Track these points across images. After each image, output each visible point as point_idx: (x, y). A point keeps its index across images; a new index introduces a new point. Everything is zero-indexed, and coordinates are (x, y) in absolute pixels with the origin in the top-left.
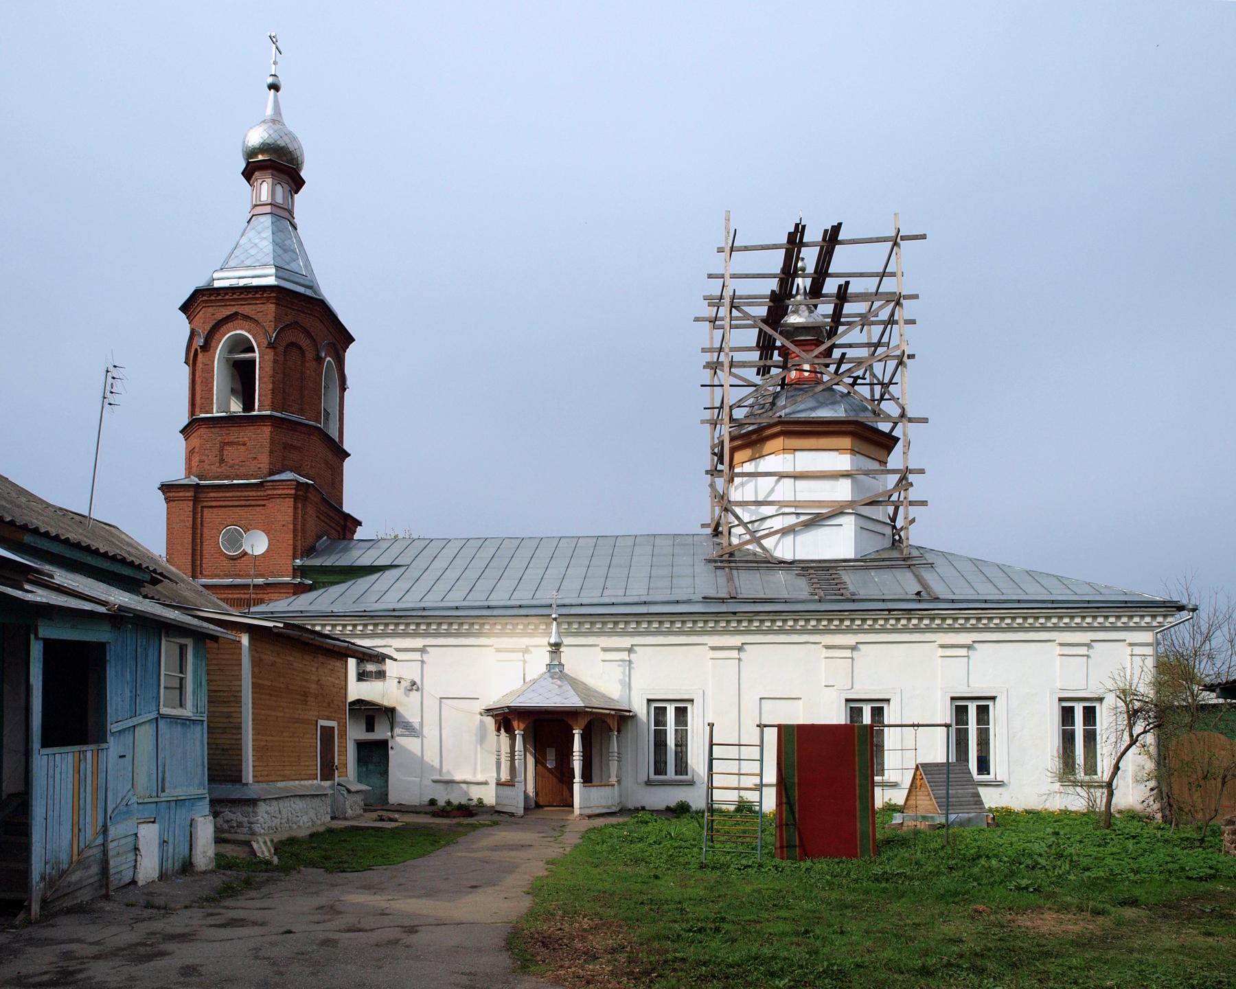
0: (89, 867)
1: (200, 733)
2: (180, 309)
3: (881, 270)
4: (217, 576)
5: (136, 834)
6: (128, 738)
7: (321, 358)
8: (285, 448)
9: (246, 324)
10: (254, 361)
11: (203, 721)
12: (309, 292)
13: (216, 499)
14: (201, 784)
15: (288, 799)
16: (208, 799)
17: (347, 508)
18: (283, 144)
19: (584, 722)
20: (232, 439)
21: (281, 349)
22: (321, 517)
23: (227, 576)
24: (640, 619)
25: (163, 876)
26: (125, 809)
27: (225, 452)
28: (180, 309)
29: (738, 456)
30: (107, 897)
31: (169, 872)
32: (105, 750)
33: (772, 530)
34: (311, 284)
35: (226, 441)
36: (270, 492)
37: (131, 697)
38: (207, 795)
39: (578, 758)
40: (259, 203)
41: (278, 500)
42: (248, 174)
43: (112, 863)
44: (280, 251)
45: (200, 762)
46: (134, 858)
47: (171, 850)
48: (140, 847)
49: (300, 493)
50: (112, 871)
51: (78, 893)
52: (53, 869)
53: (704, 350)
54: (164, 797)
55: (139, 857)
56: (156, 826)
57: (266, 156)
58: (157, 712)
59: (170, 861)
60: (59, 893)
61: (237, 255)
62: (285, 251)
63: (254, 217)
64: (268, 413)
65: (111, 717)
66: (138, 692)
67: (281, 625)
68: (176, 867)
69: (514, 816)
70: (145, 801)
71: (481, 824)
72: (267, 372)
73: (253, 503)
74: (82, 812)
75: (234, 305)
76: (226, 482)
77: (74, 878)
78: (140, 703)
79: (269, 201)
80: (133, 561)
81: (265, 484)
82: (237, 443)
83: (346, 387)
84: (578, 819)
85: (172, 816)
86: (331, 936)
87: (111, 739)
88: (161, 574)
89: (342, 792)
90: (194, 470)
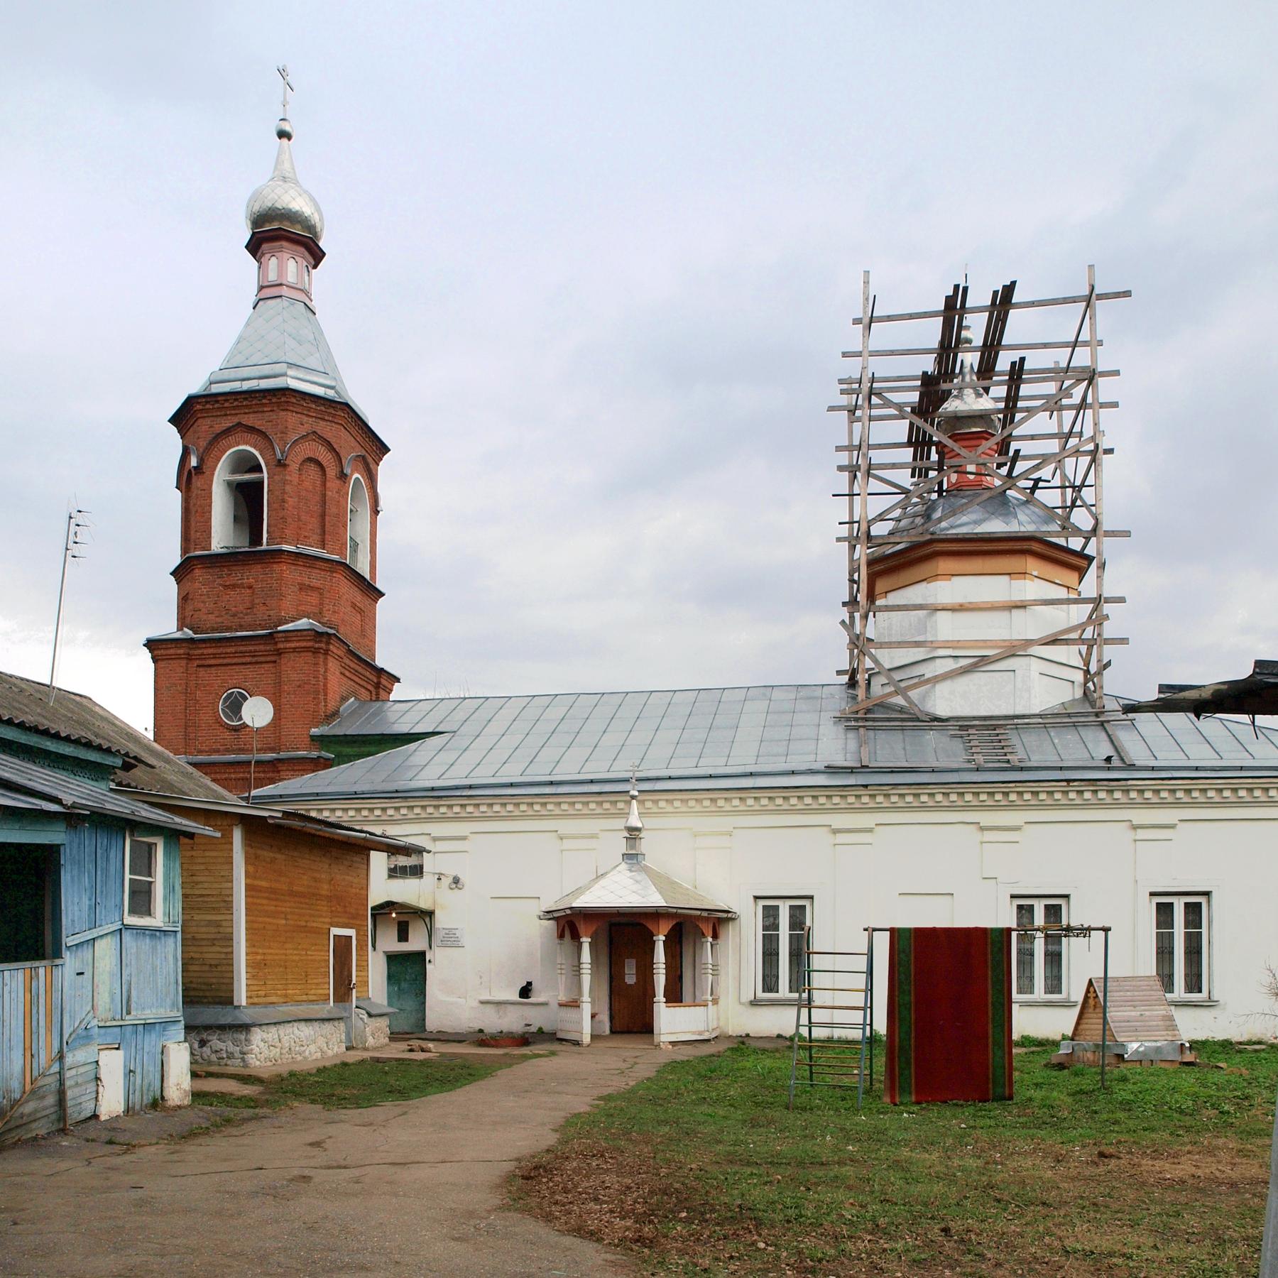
0: (43, 1097)
1: (173, 945)
2: (169, 421)
4: (217, 751)
5: (97, 1062)
6: (86, 953)
7: (346, 475)
9: (248, 436)
10: (260, 484)
11: (176, 932)
13: (215, 656)
14: (174, 1005)
16: (183, 1022)
17: (380, 662)
22: (347, 673)
23: (228, 751)
24: (743, 795)
25: (128, 1110)
26: (84, 1033)
28: (169, 421)
30: (63, 1131)
32: (60, 967)
35: (228, 583)
37: (90, 906)
38: (182, 1018)
41: (291, 654)
43: (69, 1094)
45: (172, 980)
46: (95, 1089)
47: (139, 1081)
48: (102, 1077)
50: (69, 1103)
51: (34, 1125)
52: (4, 1098)
54: (129, 1020)
55: (101, 1089)
56: (120, 1053)
58: (120, 923)
59: (138, 1093)
60: (13, 1124)
65: (66, 929)
66: (98, 900)
67: (280, 815)
68: (145, 1102)
70: (108, 1024)
74: (35, 1037)
75: (237, 414)
76: (227, 634)
77: (28, 1108)
78: (101, 913)
82: (242, 586)
83: (379, 509)
85: (139, 1042)
87: (67, 955)
90: (188, 621)
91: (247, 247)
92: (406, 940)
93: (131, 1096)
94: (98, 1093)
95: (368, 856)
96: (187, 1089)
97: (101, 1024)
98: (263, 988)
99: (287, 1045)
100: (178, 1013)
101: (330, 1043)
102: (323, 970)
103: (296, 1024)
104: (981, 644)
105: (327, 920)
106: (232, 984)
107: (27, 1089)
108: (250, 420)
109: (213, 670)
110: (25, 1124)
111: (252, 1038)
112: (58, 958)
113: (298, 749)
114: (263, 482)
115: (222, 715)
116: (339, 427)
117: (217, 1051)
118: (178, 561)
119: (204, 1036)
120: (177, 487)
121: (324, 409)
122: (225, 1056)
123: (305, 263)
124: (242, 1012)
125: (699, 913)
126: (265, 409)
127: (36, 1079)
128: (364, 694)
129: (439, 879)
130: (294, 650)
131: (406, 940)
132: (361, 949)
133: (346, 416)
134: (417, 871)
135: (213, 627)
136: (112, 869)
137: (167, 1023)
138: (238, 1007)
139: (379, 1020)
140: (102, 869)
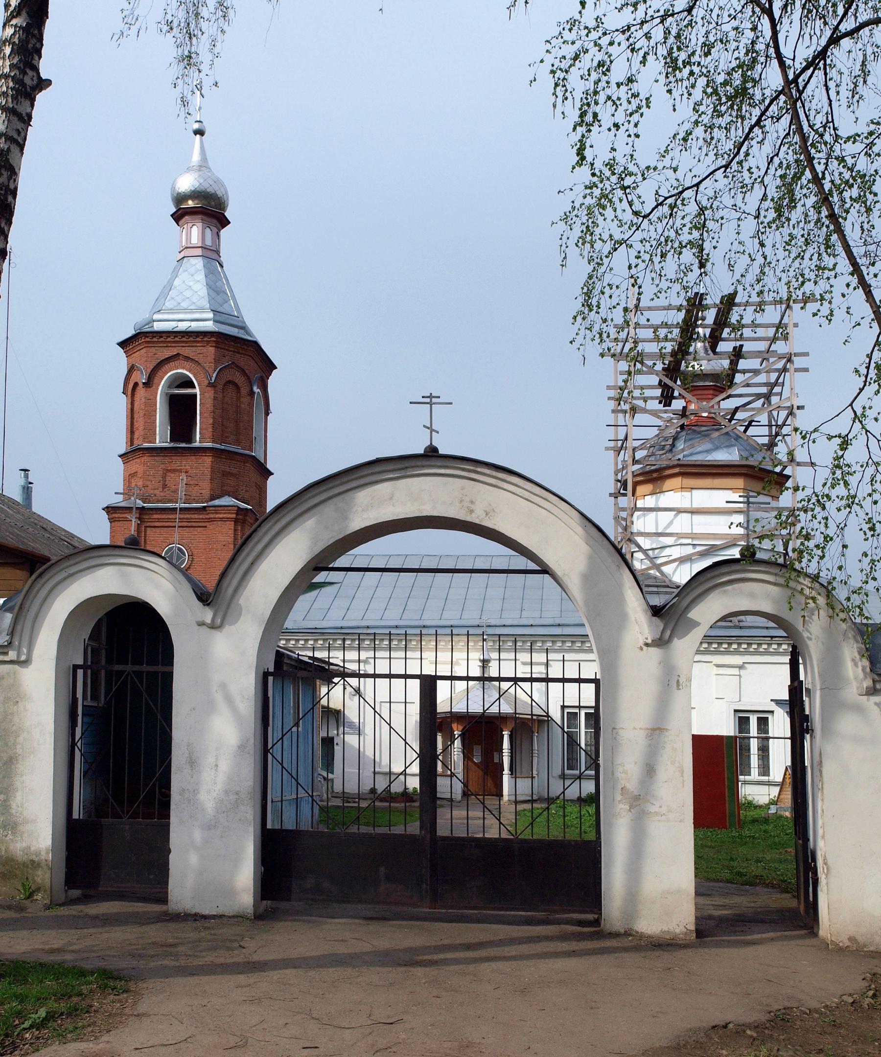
3: (777, 322)
8: (223, 475)
10: (195, 396)
12: (241, 334)
13: (159, 520)
18: (213, 192)
19: (511, 725)
20: (174, 466)
21: (220, 387)
24: (555, 639)
27: (168, 478)
29: (641, 489)
33: (671, 558)
34: (244, 325)
35: (169, 468)
36: (212, 516)
39: (507, 754)
40: (189, 245)
41: (219, 523)
42: (178, 217)
44: (214, 294)
49: (240, 517)
53: (609, 388)
57: (196, 202)
61: (173, 296)
62: (218, 293)
64: (210, 445)
72: (207, 408)
73: (194, 524)
79: (200, 245)
81: (207, 509)
104: (712, 536)
108: (187, 351)
109: (158, 530)
120: (123, 393)
130: (221, 519)
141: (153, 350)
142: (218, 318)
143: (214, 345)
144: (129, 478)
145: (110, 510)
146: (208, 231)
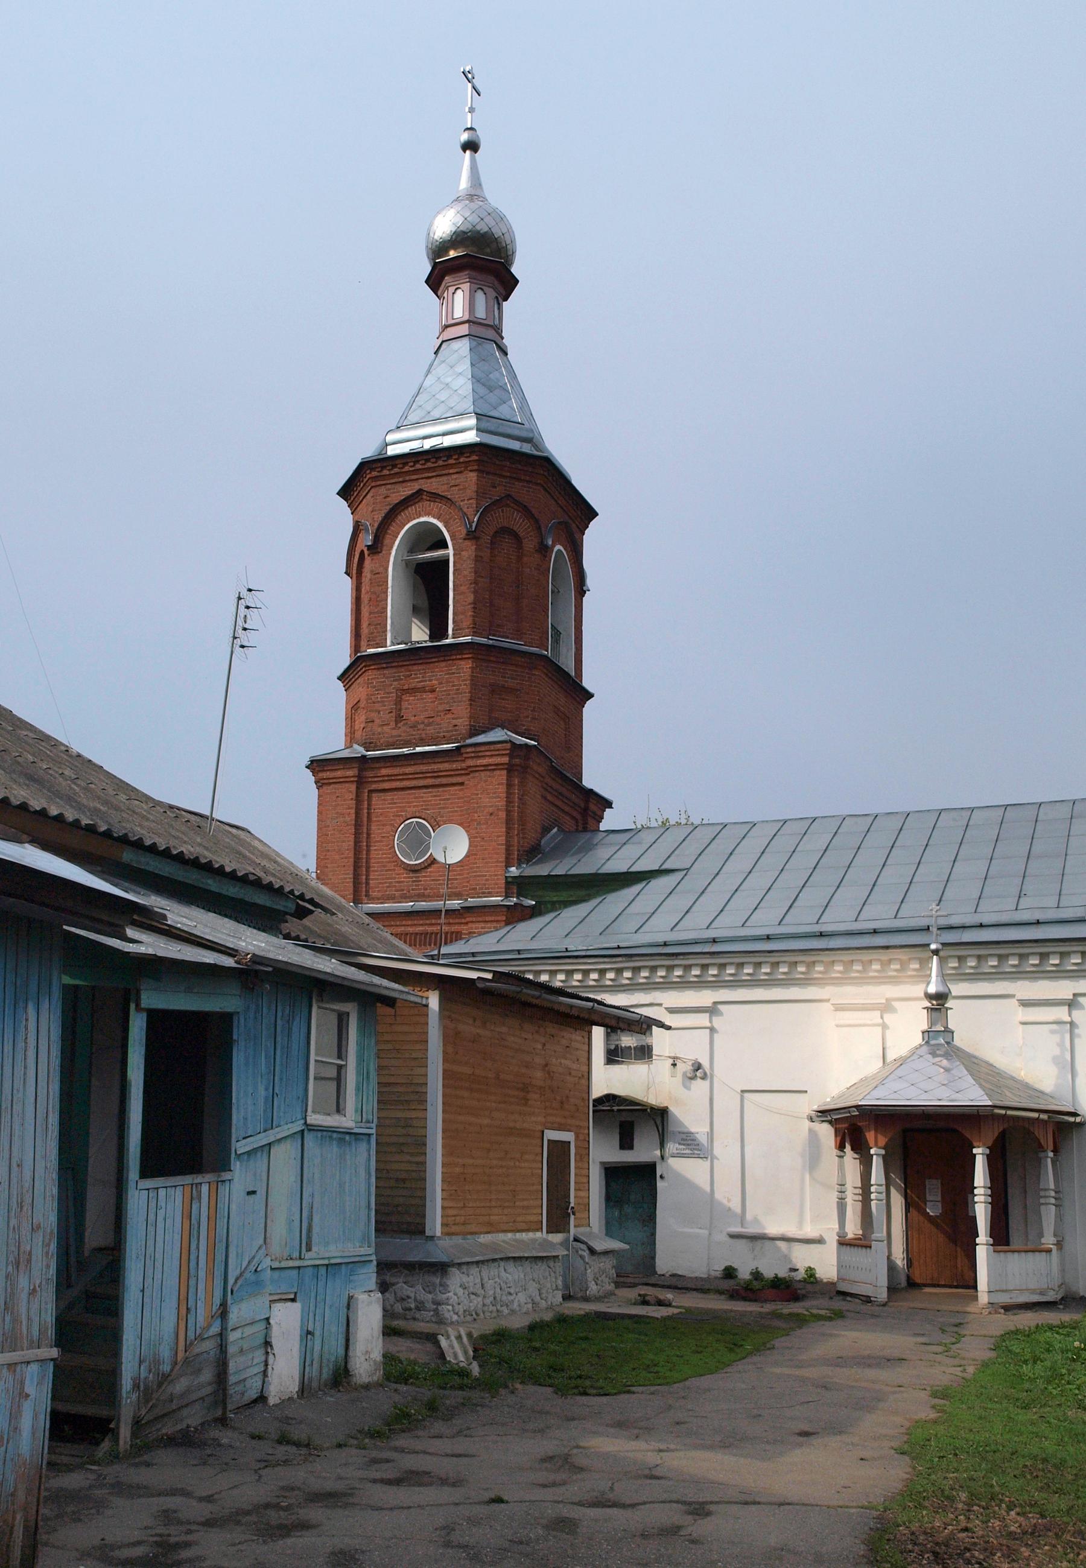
0: (200, 1370)
1: (365, 1155)
2: (338, 494)
5: (268, 1319)
6: (260, 1163)
7: (546, 547)
8: (493, 692)
9: (435, 506)
11: (369, 1135)
12: (527, 448)
14: (365, 1238)
15: (496, 1264)
16: (375, 1263)
17: (588, 782)
18: (486, 229)
20: (414, 683)
21: (486, 539)
22: (549, 797)
25: (304, 1389)
26: (253, 1278)
27: (405, 705)
28: (338, 494)
30: (222, 1421)
31: (315, 1385)
32: (227, 1184)
34: (531, 435)
35: (406, 687)
36: (470, 763)
38: (374, 1258)
40: (451, 322)
41: (482, 774)
42: (435, 282)
43: (232, 1366)
44: (482, 391)
45: (364, 1203)
46: (263, 1358)
47: (317, 1348)
48: (274, 1342)
49: (517, 761)
50: (232, 1379)
51: (185, 1412)
52: (150, 1371)
54: (311, 1258)
55: (271, 1358)
56: (297, 1306)
57: (460, 250)
58: (303, 1122)
59: (316, 1365)
60: (158, 1411)
61: (420, 404)
62: (491, 389)
63: (444, 344)
64: (468, 639)
67: (489, 976)
68: (325, 1376)
69: (871, 1302)
70: (284, 1264)
71: (813, 1315)
72: (465, 576)
73: (444, 781)
74: (192, 1282)
75: (417, 479)
76: (405, 750)
77: (180, 1386)
79: (466, 318)
80: (271, 882)
81: (463, 750)
82: (423, 690)
83: (585, 588)
84: (985, 1312)
85: (321, 1290)
86: (567, 1511)
87: (236, 1165)
88: (311, 901)
89: (580, 1252)
91: (427, 282)
92: (631, 1148)
93: (307, 1369)
94: (266, 1365)
95: (590, 1032)
96: (378, 1359)
97: (276, 1265)
98: (462, 1212)
99: (491, 1292)
100: (368, 1251)
101: (544, 1291)
102: (535, 1187)
103: (502, 1264)
105: (541, 1119)
106: (424, 1206)
107: (179, 1359)
108: (434, 485)
110: (174, 1411)
111: (449, 1282)
112: (225, 1171)
113: (490, 895)
114: (448, 560)
115: (398, 852)
116: (538, 488)
117: (403, 1299)
118: (346, 662)
119: (388, 1278)
121: (520, 467)
122: (413, 1306)
123: (495, 294)
124: (436, 1245)
125: (1035, 1115)
126: (451, 471)
127: (191, 1344)
128: (570, 824)
129: (674, 1065)
130: (486, 768)
131: (631, 1148)
132: (581, 1160)
133: (546, 474)
134: (644, 1053)
135: (388, 742)
136: (295, 1046)
137: (355, 1264)
138: (432, 1238)
139: (603, 1259)
140: (282, 1048)
141: (383, 490)
142: (485, 425)
143: (476, 467)
144: (353, 710)
145: (317, 765)
146: (480, 297)
